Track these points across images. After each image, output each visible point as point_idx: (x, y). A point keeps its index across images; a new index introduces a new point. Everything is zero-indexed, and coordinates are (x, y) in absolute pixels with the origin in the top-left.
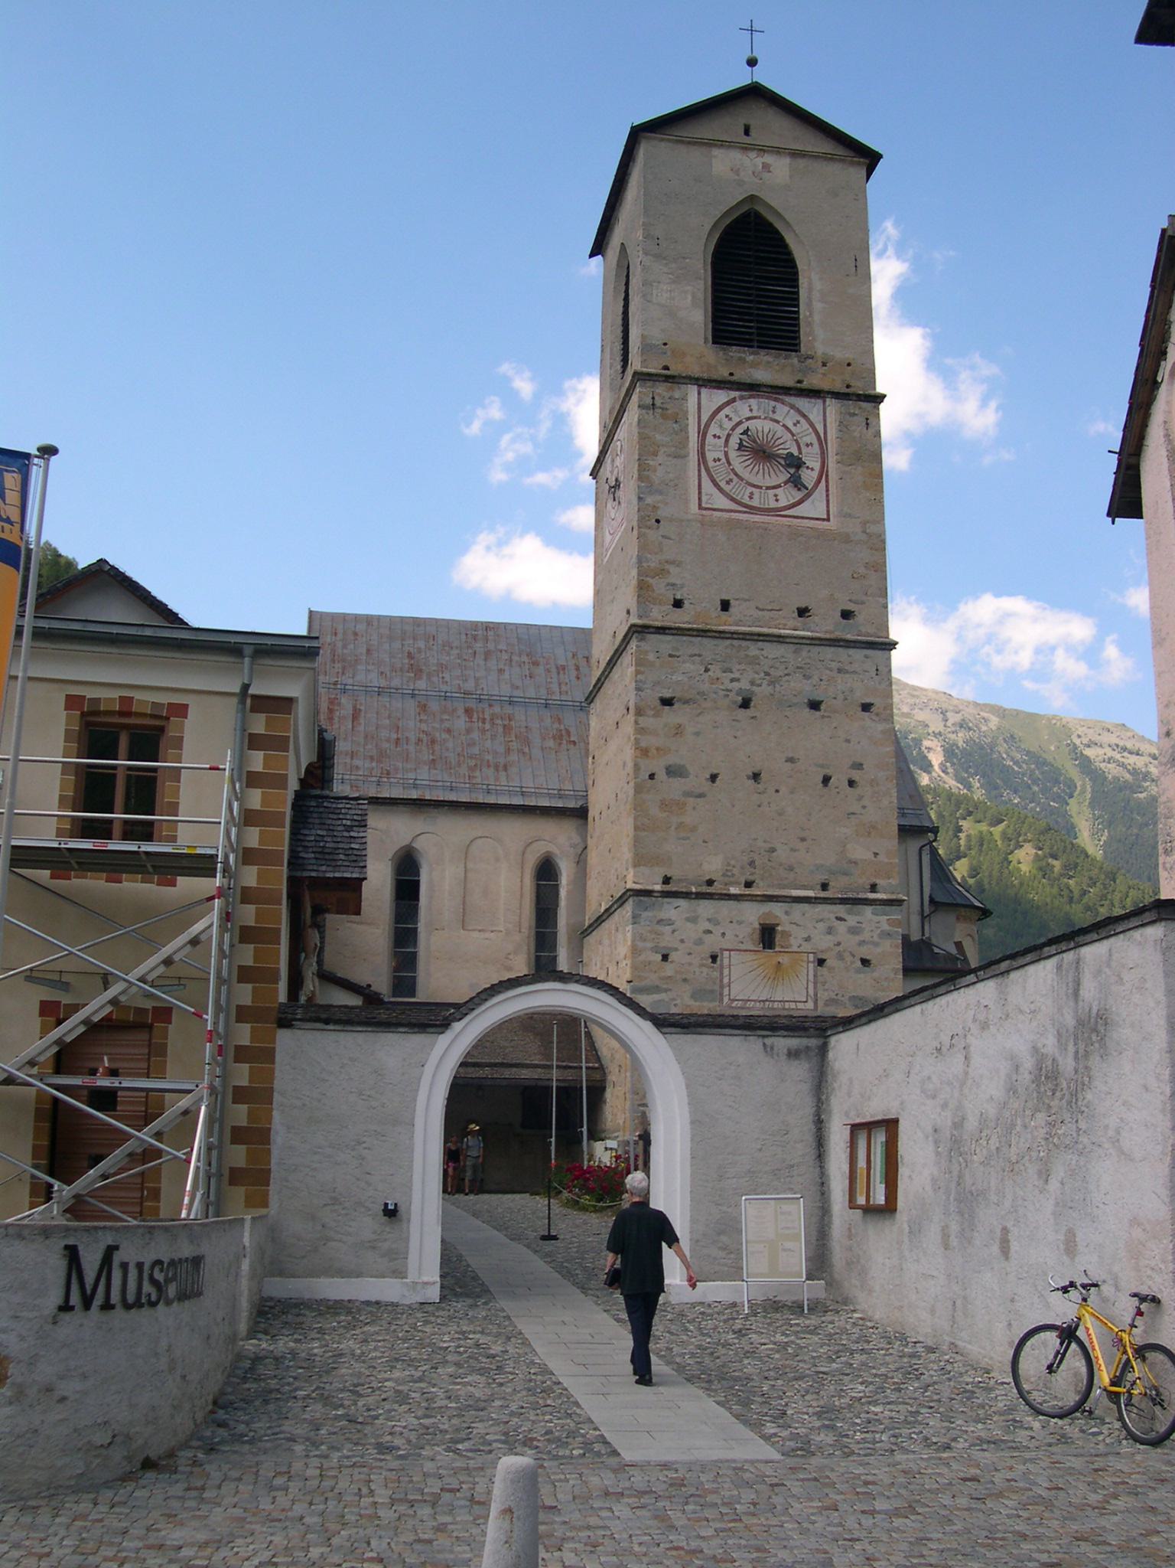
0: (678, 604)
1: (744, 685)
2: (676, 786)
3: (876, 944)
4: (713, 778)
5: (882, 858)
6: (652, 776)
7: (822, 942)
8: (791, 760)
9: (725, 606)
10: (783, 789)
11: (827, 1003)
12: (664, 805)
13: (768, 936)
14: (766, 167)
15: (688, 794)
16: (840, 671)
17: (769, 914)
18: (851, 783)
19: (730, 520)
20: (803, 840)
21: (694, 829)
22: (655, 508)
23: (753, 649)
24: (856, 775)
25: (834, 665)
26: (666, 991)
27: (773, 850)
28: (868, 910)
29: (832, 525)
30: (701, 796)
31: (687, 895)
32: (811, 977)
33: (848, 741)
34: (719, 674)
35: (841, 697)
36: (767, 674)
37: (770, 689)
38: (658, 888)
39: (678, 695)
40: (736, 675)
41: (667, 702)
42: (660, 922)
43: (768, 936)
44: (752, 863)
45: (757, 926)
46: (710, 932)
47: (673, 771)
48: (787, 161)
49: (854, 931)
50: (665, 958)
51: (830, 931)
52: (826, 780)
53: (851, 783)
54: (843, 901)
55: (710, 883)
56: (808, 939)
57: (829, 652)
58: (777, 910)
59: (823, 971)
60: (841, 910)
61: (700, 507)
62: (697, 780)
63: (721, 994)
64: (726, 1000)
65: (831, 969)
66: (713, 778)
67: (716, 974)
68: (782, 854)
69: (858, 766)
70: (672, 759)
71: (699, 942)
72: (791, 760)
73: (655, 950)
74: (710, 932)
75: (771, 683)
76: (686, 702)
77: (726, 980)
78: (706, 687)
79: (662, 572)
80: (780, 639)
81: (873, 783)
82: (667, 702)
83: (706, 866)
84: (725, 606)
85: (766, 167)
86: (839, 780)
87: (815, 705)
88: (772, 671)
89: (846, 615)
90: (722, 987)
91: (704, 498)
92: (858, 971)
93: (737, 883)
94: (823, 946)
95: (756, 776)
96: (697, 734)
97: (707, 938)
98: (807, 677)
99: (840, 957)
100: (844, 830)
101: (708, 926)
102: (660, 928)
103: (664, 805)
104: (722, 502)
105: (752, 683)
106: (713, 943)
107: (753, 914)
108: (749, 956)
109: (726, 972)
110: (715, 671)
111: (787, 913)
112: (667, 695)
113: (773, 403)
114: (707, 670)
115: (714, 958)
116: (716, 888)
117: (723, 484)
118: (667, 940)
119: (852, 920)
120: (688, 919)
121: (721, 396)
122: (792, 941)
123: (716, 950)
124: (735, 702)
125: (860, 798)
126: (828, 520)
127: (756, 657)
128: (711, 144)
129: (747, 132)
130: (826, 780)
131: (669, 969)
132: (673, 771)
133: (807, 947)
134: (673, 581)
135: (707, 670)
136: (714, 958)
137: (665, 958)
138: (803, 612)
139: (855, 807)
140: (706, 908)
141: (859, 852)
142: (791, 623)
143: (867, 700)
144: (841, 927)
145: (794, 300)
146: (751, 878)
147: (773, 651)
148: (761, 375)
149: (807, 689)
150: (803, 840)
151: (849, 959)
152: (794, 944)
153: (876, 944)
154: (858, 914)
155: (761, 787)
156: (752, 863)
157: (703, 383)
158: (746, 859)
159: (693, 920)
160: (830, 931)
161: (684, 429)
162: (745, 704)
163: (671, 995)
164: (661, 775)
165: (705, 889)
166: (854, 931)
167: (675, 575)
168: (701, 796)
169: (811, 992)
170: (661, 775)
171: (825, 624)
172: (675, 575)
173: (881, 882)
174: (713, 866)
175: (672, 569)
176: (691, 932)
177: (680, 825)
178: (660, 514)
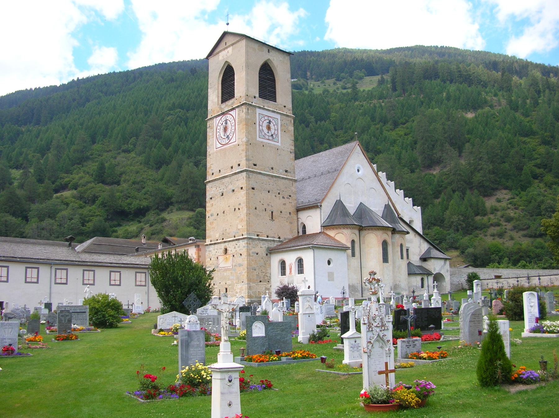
1: (222, 190)
10: (228, 214)
13: (226, 250)
23: (224, 180)
27: (226, 230)
28: (241, 241)
48: (231, 47)
51: (235, 248)
58: (226, 244)
59: (234, 258)
71: (215, 255)
72: (229, 206)
86: (237, 209)
97: (217, 253)
99: (236, 254)
101: (216, 250)
105: (223, 189)
107: (223, 246)
108: (222, 256)
113: (227, 115)
147: (227, 179)
166: (239, 247)
177: (213, 227)
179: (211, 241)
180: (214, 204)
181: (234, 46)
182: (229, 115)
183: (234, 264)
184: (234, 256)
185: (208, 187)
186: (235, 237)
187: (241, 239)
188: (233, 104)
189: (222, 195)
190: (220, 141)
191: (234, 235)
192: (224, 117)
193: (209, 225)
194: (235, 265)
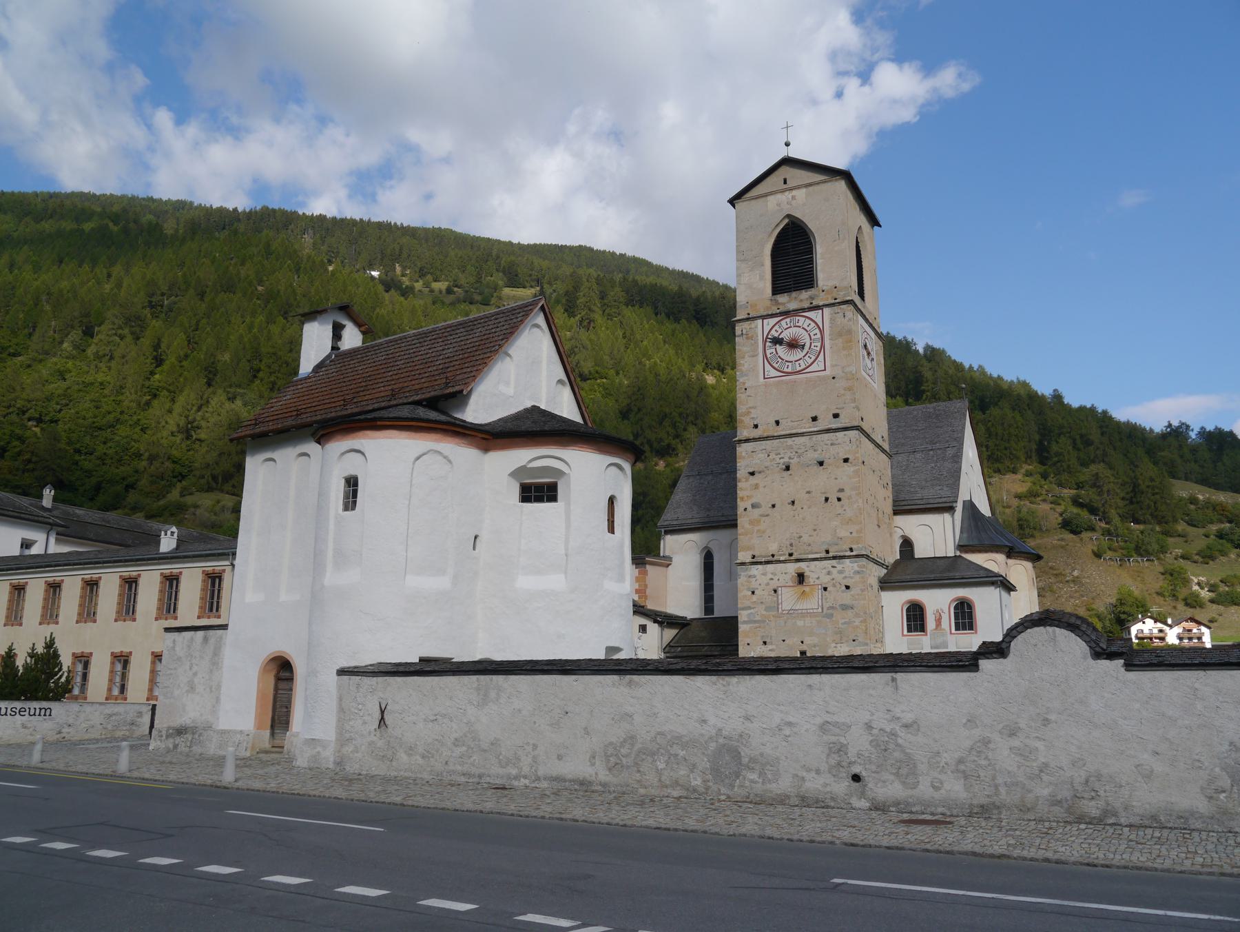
0: (756, 426)
1: (786, 460)
2: (757, 512)
3: (851, 578)
4: (774, 506)
5: (854, 534)
6: (745, 509)
7: (825, 580)
8: (808, 492)
9: (777, 423)
10: (805, 507)
11: (828, 609)
12: (751, 523)
13: (801, 578)
14: (793, 198)
15: (762, 516)
16: (832, 444)
17: (799, 568)
18: (839, 499)
19: (779, 381)
20: (815, 530)
21: (764, 532)
22: (744, 383)
23: (789, 441)
24: (840, 495)
25: (829, 442)
26: (754, 608)
27: (800, 537)
28: (847, 561)
29: (828, 372)
30: (767, 515)
31: (761, 563)
32: (820, 597)
33: (836, 479)
34: (774, 456)
35: (832, 457)
36: (796, 452)
37: (798, 460)
38: (748, 561)
39: (756, 470)
40: (782, 456)
41: (752, 474)
42: (750, 577)
43: (801, 578)
44: (791, 545)
45: (794, 574)
46: (772, 579)
47: (753, 506)
48: (804, 190)
49: (840, 572)
50: (753, 593)
51: (829, 573)
52: (827, 499)
53: (839, 499)
54: (834, 558)
55: (773, 556)
56: (818, 578)
57: (826, 436)
58: (803, 565)
60: (834, 562)
61: (764, 378)
62: (766, 508)
63: (778, 608)
64: (780, 610)
65: (830, 592)
66: (774, 506)
67: (775, 599)
68: (805, 538)
69: (841, 490)
70: (754, 500)
71: (768, 584)
72: (808, 492)
73: (748, 589)
74: (772, 579)
75: (799, 456)
76: (760, 472)
77: (780, 601)
78: (767, 464)
79: (749, 413)
80: (802, 434)
81: (849, 498)
82: (752, 474)
83: (770, 549)
84: (777, 423)
85: (793, 198)
86: (833, 499)
87: (821, 464)
88: (799, 451)
89: (836, 416)
90: (778, 605)
91: (766, 373)
92: (843, 592)
93: (784, 555)
94: (826, 581)
95: (793, 502)
96: (765, 487)
98: (815, 450)
99: (834, 586)
100: (835, 523)
101: (771, 576)
102: (751, 579)
103: (751, 523)
104: (774, 373)
105: (790, 458)
106: (774, 584)
107: (792, 568)
108: (792, 589)
109: (780, 597)
110: (772, 456)
111: (808, 567)
112: (751, 471)
113: (797, 318)
114: (769, 456)
115: (775, 591)
116: (776, 558)
117: (774, 365)
118: (754, 585)
119: (839, 567)
120: (763, 574)
121: (773, 321)
122: (811, 580)
123: (775, 587)
124: (781, 469)
125: (842, 506)
126: (825, 370)
127: (791, 445)
128: (766, 195)
129: (785, 182)
130: (827, 499)
131: (754, 598)
132: (753, 506)
133: (818, 582)
134: (752, 416)
135: (769, 456)
136: (775, 591)
137: (753, 593)
138: (814, 419)
139: (840, 511)
140: (769, 566)
141: (843, 533)
142: (808, 425)
143: (846, 457)
144: (834, 571)
145: (810, 261)
146: (791, 552)
148: (793, 306)
149: (817, 456)
150: (815, 530)
151: (838, 586)
152: (811, 581)
153: (851, 578)
154: (843, 563)
155: (794, 508)
156: (791, 545)
157: (763, 317)
158: (788, 543)
159: (764, 574)
160: (829, 573)
161: (756, 342)
162: (788, 468)
163: (756, 610)
164: (749, 508)
165: (770, 558)
166: (840, 572)
167: (754, 413)
168: (767, 515)
169: (820, 604)
170: (749, 508)
171: (826, 422)
172: (754, 413)
173: (853, 547)
174: (773, 548)
175: (752, 411)
176: (765, 580)
177: (758, 531)
178: (746, 386)
179: (754, 557)
180: (761, 485)
181: (811, 188)
182: (802, 319)
183: (826, 605)
184: (825, 589)
185: (742, 450)
186: (827, 552)
187: (849, 557)
188: (812, 298)
189: (788, 468)
190: (776, 366)
191: (825, 547)
192: (788, 320)
193: (747, 526)
194: (832, 608)
